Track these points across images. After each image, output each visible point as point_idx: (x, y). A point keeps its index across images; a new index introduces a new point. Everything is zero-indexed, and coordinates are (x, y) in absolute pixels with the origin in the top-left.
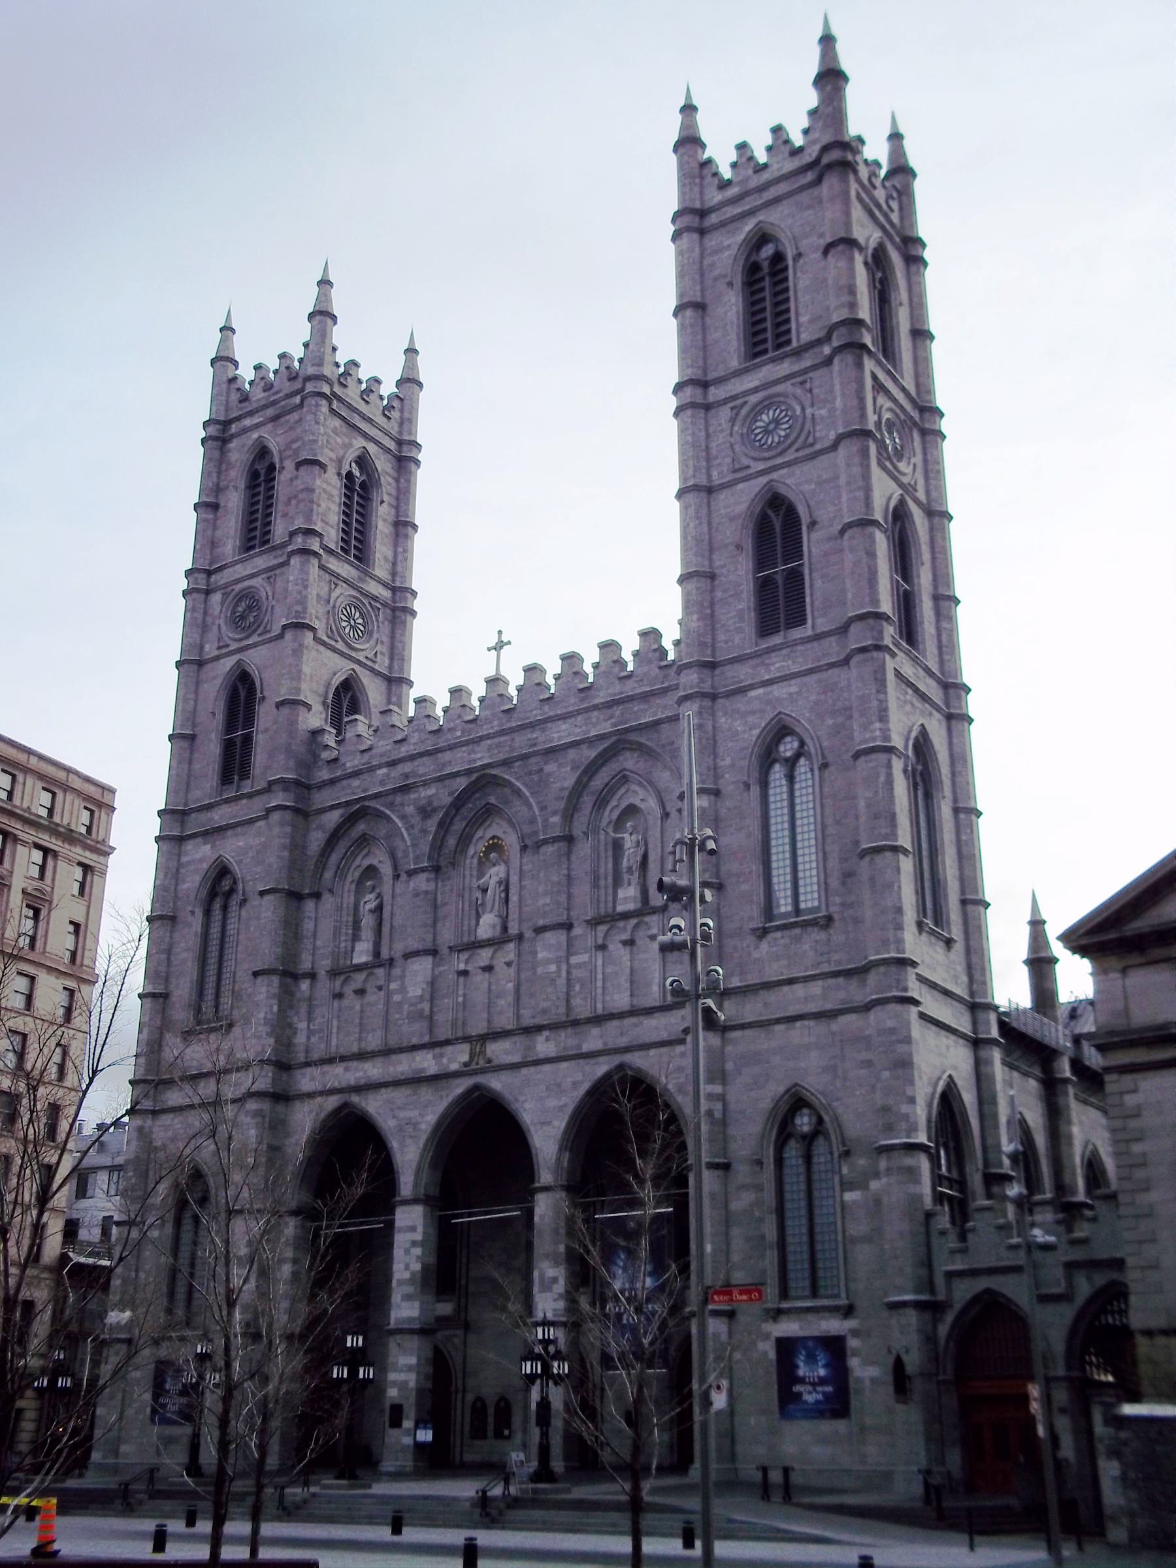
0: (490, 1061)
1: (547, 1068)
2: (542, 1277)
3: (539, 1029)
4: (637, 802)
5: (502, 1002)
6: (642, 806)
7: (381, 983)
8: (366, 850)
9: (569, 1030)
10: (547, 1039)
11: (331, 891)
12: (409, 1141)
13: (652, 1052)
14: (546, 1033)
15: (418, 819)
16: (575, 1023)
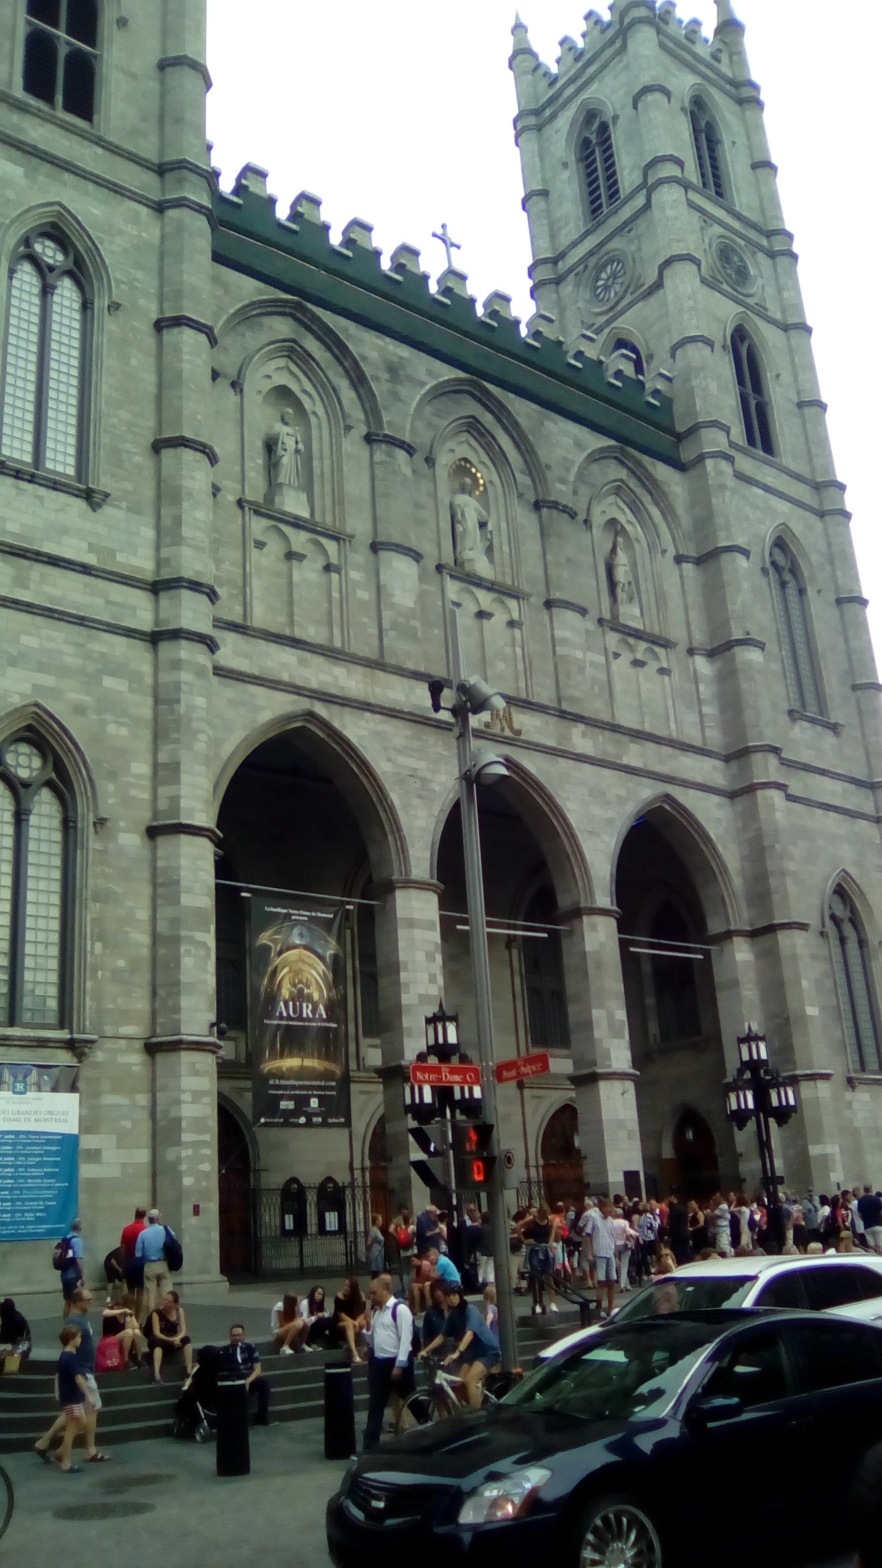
0: (518, 733)
1: (587, 767)
2: (610, 1017)
3: (578, 718)
4: (622, 519)
5: (501, 666)
6: (628, 528)
7: (334, 560)
8: (282, 362)
9: (607, 733)
10: (584, 735)
11: (234, 385)
12: (416, 801)
13: (691, 791)
14: (581, 727)
15: (385, 376)
16: (615, 728)
